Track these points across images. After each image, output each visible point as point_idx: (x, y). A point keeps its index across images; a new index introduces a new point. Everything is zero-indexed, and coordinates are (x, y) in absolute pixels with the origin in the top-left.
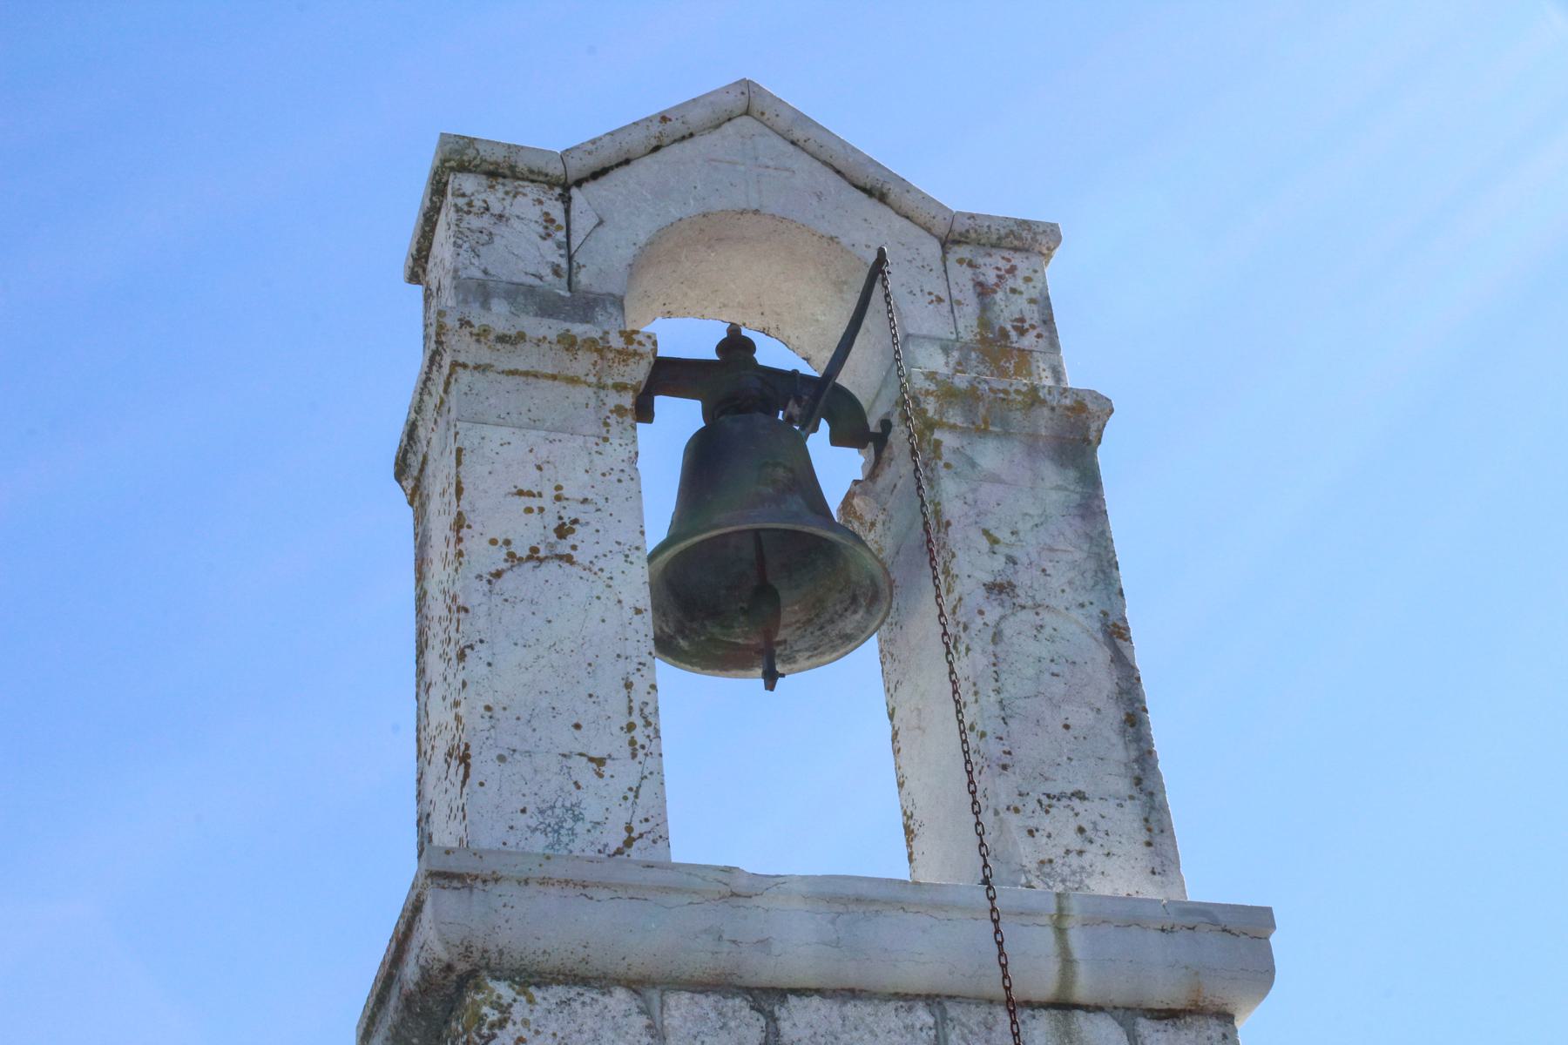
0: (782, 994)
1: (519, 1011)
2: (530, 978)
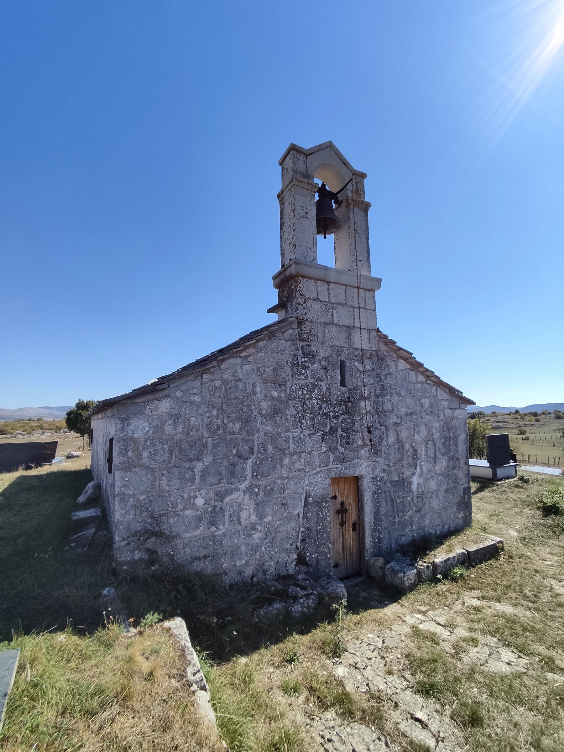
0: (330, 282)
1: (302, 281)
2: (303, 277)
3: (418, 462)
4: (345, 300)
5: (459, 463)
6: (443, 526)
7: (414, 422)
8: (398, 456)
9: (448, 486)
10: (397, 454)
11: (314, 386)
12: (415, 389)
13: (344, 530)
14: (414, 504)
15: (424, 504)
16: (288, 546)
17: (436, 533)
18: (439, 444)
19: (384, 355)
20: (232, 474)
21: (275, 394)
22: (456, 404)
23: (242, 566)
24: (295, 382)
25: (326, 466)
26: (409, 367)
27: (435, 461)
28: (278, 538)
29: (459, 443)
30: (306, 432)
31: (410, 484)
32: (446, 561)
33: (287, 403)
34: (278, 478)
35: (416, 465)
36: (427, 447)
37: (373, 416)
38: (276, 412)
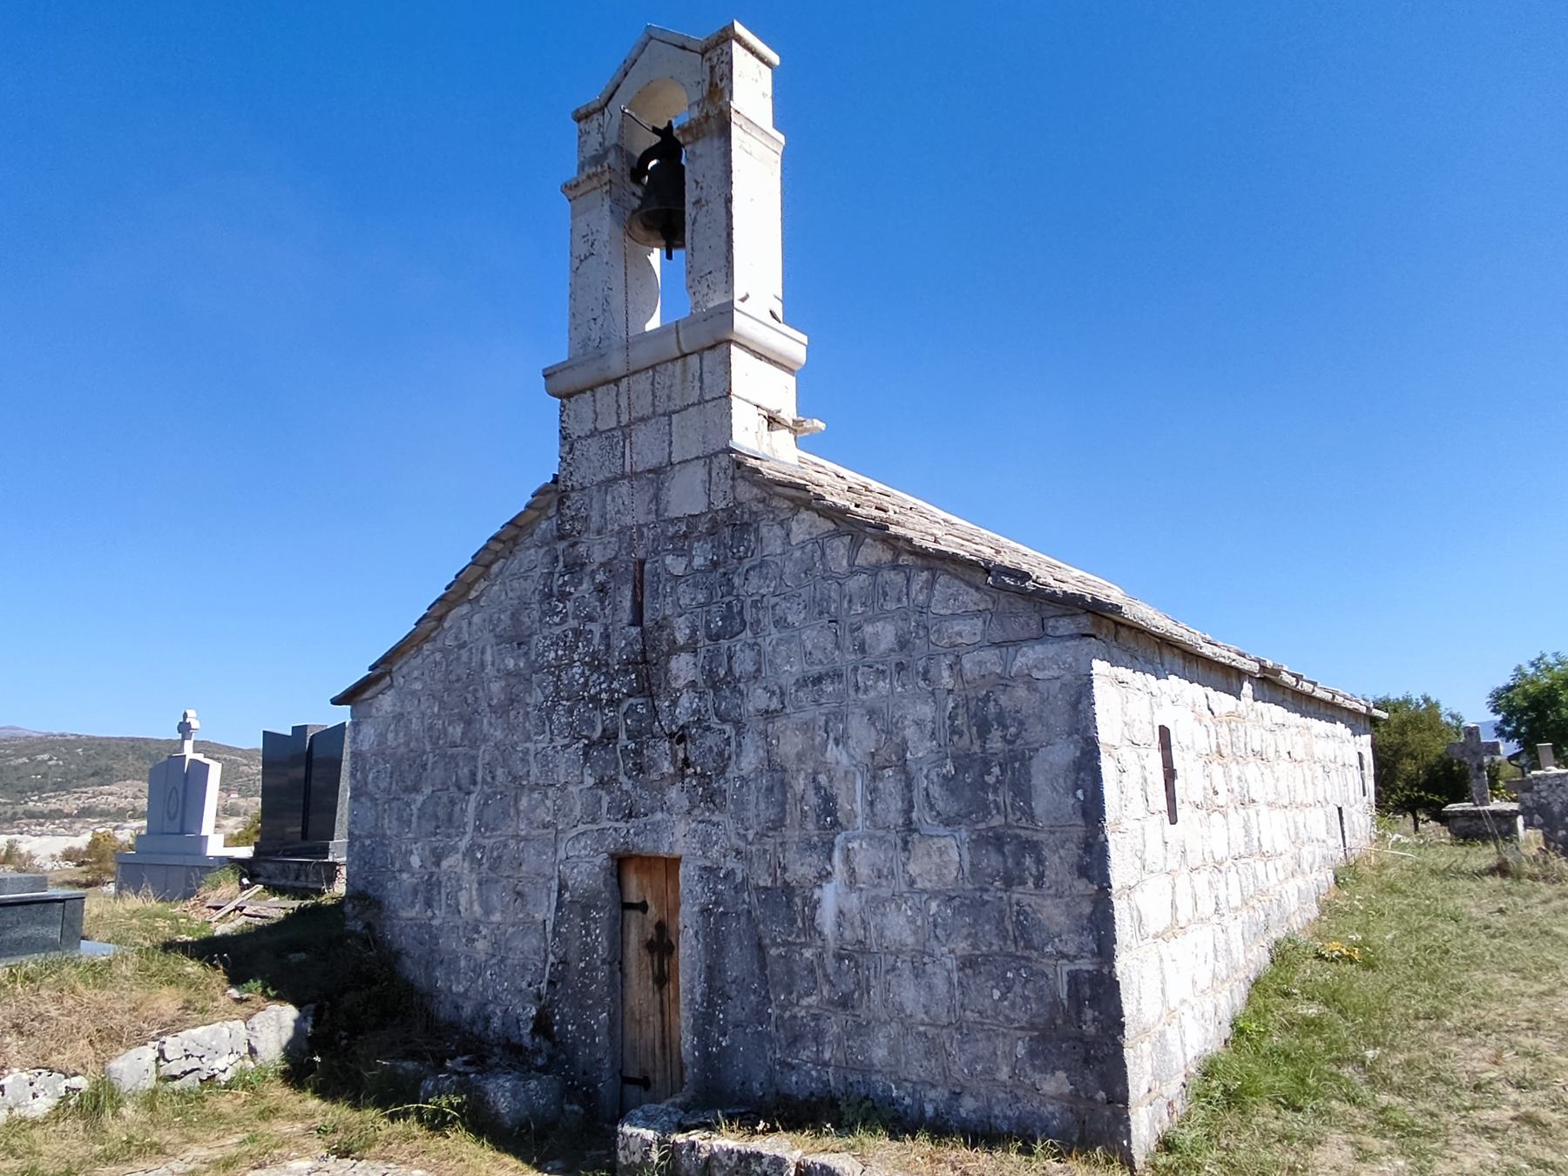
3: (839, 839)
4: (653, 405)
5: (1040, 861)
6: (956, 1095)
7: (831, 706)
9: (975, 946)
10: (762, 806)
11: (577, 633)
12: (842, 596)
13: (665, 998)
14: (826, 976)
16: (524, 985)
17: (922, 1111)
19: (751, 513)
20: (450, 819)
21: (511, 663)
22: (1023, 621)
23: (459, 994)
24: (546, 632)
25: (594, 821)
26: (832, 526)
27: (906, 843)
28: (509, 961)
29: (1039, 780)
30: (559, 741)
32: (747, 1158)
33: (529, 681)
34: (513, 837)
35: (829, 848)
36: (874, 790)
38: (512, 700)
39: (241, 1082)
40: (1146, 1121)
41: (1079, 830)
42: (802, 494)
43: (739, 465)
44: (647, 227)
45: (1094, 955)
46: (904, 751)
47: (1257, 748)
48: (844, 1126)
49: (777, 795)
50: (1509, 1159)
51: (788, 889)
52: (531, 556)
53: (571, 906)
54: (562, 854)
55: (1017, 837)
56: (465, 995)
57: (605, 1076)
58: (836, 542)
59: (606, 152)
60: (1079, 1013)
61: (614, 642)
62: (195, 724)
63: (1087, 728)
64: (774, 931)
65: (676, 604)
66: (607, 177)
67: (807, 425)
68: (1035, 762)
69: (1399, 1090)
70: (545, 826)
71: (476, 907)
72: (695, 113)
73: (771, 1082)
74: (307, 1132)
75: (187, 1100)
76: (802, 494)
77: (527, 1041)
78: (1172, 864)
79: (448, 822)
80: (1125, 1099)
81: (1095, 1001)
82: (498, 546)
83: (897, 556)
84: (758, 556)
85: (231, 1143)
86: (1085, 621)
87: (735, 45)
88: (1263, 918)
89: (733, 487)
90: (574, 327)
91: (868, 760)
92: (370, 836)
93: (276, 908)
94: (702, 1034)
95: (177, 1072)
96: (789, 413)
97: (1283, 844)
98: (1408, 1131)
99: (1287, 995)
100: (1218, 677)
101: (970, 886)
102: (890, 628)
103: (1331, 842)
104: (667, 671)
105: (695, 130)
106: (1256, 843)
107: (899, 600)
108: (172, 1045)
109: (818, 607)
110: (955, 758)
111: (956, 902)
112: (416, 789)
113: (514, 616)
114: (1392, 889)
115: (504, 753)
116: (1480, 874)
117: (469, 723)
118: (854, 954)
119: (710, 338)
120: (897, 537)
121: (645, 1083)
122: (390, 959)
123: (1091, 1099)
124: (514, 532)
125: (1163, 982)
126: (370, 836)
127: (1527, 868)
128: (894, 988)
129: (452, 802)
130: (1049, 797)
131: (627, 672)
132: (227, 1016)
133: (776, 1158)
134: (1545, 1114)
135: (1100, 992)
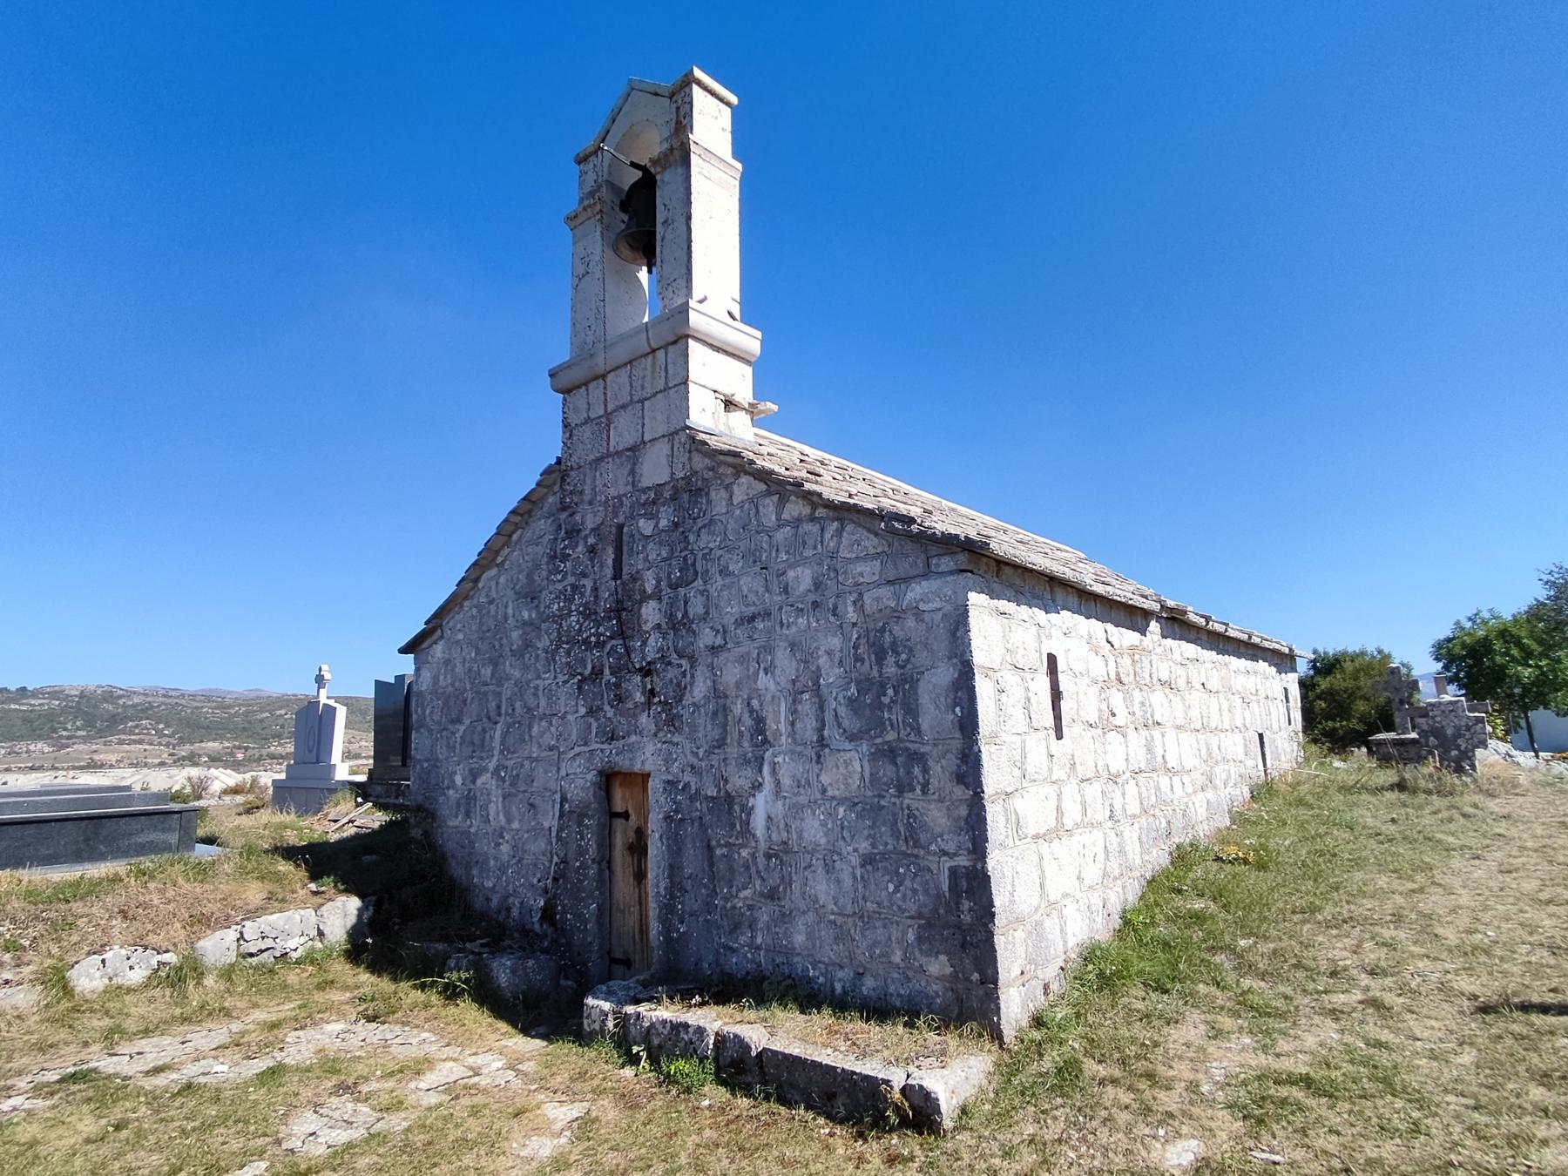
5: (925, 771)
6: (860, 975)
8: (715, 734)
9: (874, 846)
10: (709, 728)
14: (758, 872)
15: (787, 882)
17: (833, 990)
18: (836, 703)
19: (704, 480)
21: (526, 615)
25: (586, 744)
26: (764, 487)
27: (819, 756)
29: (925, 699)
31: (749, 811)
33: (539, 628)
36: (796, 711)
37: (664, 636)
38: (528, 645)
39: (309, 959)
40: (1018, 1000)
41: (957, 743)
42: (738, 461)
43: (693, 439)
44: (633, 248)
45: (969, 852)
46: (818, 677)
47: (1165, 678)
48: (761, 1001)
49: (721, 719)
50: (1348, 1038)
51: (730, 798)
52: (542, 525)
53: (571, 815)
54: (563, 773)
55: (907, 749)
56: (492, 889)
57: (594, 957)
58: (767, 501)
59: (600, 187)
60: (958, 904)
61: (601, 594)
62: (327, 676)
63: (964, 653)
64: (719, 834)
65: (646, 560)
66: (598, 207)
67: (761, 407)
68: (921, 683)
69: (1263, 976)
70: (551, 749)
71: (501, 817)
72: (666, 146)
73: (717, 961)
74: (351, 1001)
75: (261, 972)
76: (738, 461)
77: (537, 926)
78: (1059, 774)
79: (480, 747)
80: (995, 982)
81: (971, 893)
82: (517, 519)
83: (814, 509)
84: (708, 516)
85: (289, 1008)
86: (962, 559)
87: (695, 87)
88: (1164, 824)
89: (690, 459)
90: (575, 334)
91: (789, 686)
92: (427, 760)
93: (372, 819)
94: (664, 921)
95: (254, 950)
96: (744, 395)
97: (1191, 761)
98: (1262, 1012)
99: (1180, 891)
100: (1122, 614)
101: (869, 793)
102: (808, 571)
103: (1250, 763)
104: (640, 616)
105: (663, 161)
106: (1160, 760)
107: (815, 548)
108: (250, 929)
109: (752, 557)
110: (858, 683)
111: (859, 808)
112: (459, 721)
113: (529, 576)
114: (1301, 802)
115: (521, 686)
116: (1380, 790)
117: (496, 665)
118: (780, 853)
119: (674, 335)
120: (811, 493)
121: (627, 963)
122: (439, 860)
123: (968, 980)
124: (529, 506)
125: (1042, 877)
126: (427, 760)
127: (1422, 783)
128: (810, 882)
129: (484, 731)
130: (934, 715)
131: (610, 619)
132: (303, 904)
133: (699, 1027)
134: (1390, 999)
135: (974, 885)
